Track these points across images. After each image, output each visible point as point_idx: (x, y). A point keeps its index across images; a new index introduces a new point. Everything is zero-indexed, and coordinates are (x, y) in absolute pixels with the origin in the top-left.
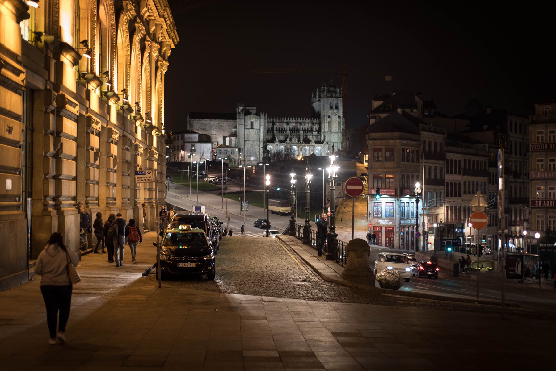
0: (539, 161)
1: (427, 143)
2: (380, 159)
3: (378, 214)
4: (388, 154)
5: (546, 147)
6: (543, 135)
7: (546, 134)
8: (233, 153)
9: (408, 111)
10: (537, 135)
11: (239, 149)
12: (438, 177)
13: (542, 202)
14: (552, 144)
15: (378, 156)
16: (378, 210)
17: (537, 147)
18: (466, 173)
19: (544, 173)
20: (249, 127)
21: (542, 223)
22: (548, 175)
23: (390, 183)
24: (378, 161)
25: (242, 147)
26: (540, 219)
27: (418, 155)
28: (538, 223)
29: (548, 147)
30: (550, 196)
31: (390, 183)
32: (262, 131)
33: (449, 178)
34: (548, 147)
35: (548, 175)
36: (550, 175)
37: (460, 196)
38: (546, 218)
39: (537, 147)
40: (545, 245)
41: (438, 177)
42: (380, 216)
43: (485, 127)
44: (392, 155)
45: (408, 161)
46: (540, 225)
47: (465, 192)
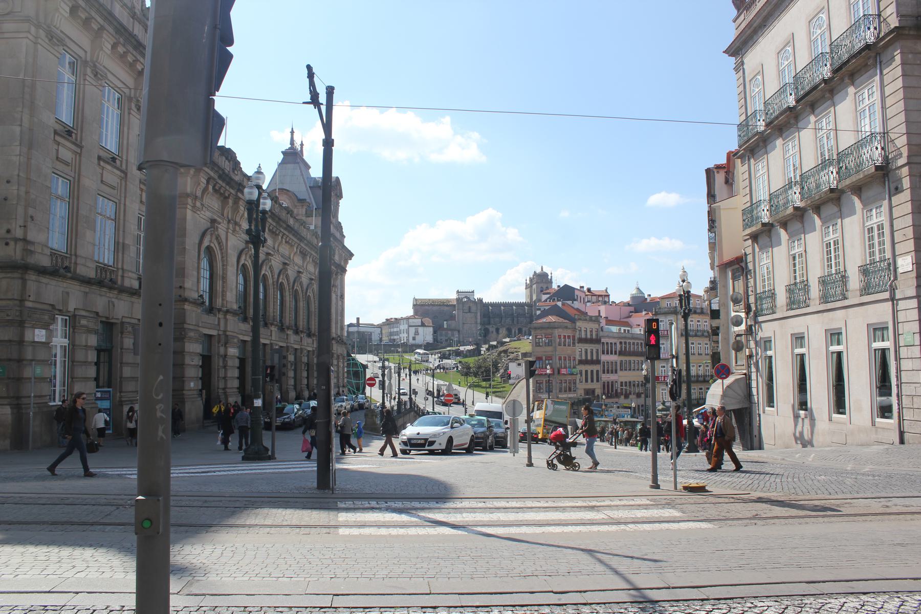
1: (583, 329)
8: (453, 335)
9: (570, 302)
12: (595, 358)
18: (621, 353)
27: (574, 339)
32: (479, 314)
33: (604, 358)
37: (616, 372)
41: (595, 358)
44: (550, 341)
45: (565, 345)
47: (621, 370)
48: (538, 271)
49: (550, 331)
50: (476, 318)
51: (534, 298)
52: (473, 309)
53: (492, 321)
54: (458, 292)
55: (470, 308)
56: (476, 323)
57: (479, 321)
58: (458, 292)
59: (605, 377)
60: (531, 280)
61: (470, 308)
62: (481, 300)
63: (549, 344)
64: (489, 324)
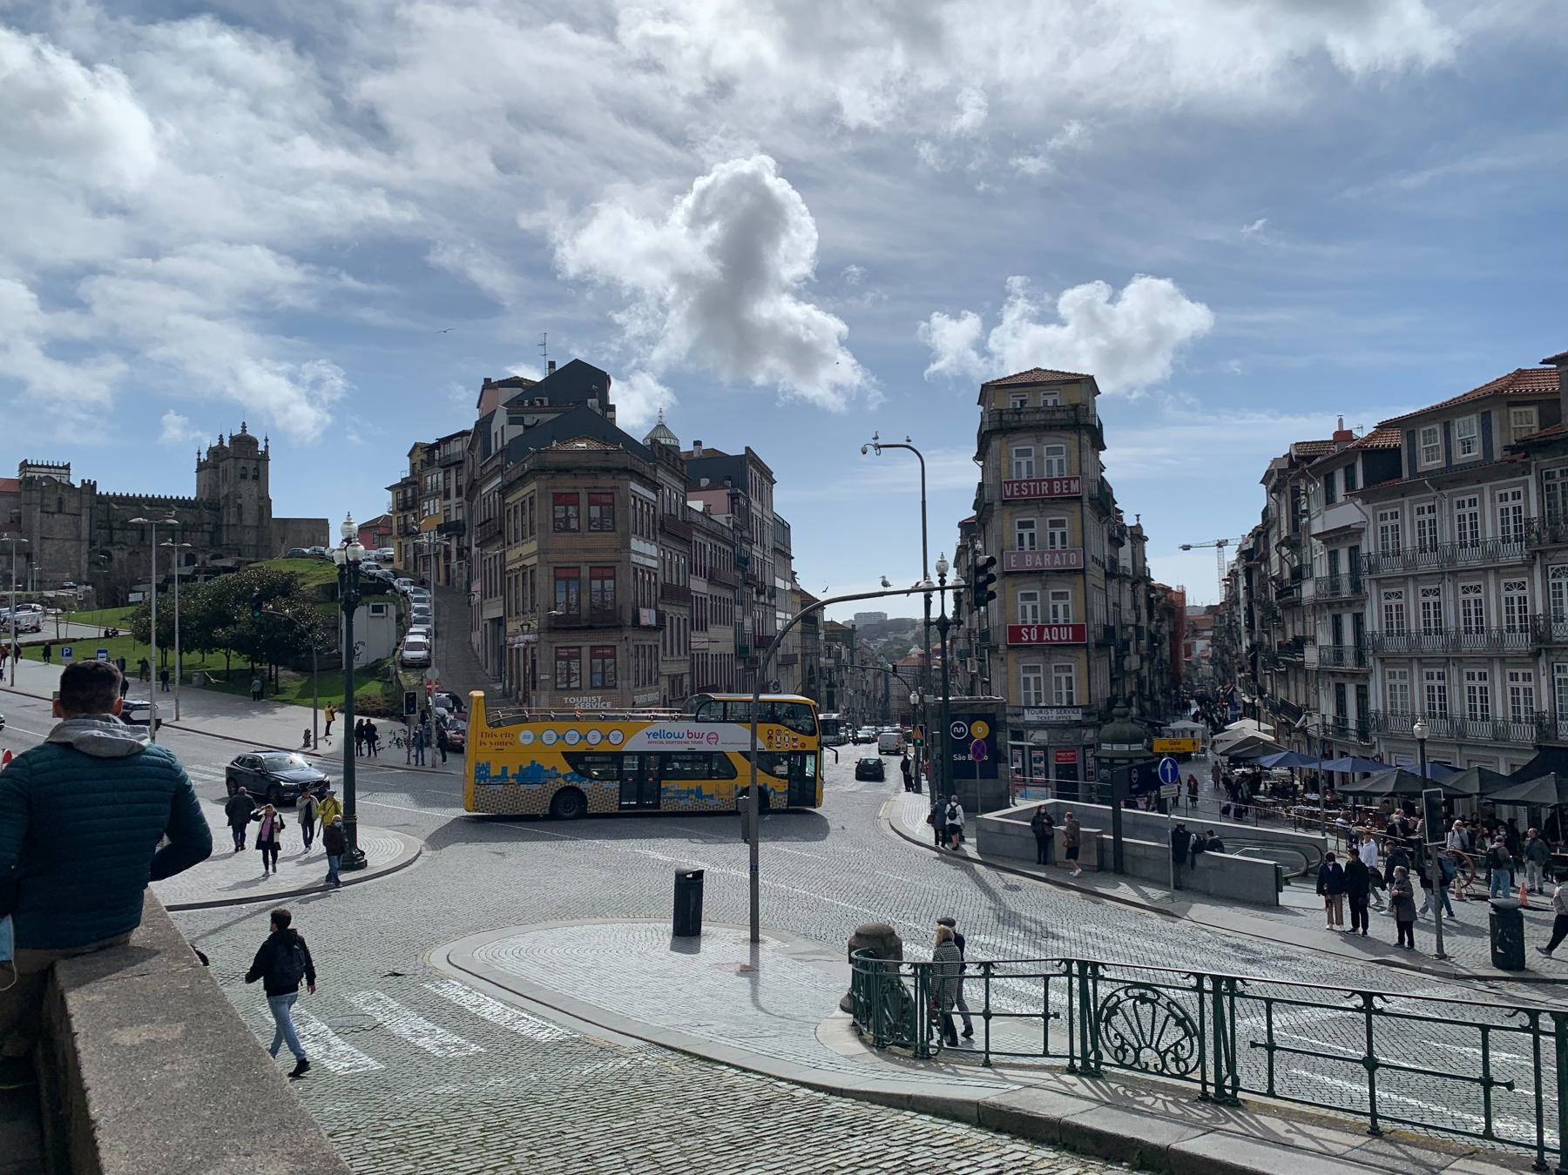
0: (1022, 525)
2: (574, 524)
3: (568, 682)
4: (595, 512)
5: (1045, 488)
6: (1032, 459)
7: (1039, 457)
10: (1015, 459)
11: (29, 556)
13: (1041, 630)
14: (1060, 480)
15: (568, 518)
16: (569, 668)
17: (1020, 490)
19: (1042, 557)
20: (53, 508)
21: (1038, 687)
22: (1053, 559)
23: (603, 590)
24: (567, 529)
25: (36, 550)
26: (1032, 677)
28: (1027, 686)
29: (1051, 489)
30: (1055, 614)
31: (603, 590)
32: (85, 519)
34: (1051, 489)
35: (1053, 559)
36: (1057, 561)
38: (1047, 672)
39: (1020, 490)
40: (1126, 747)
42: (575, 684)
43: (705, 482)
46: (1064, 691)
48: (237, 431)
49: (605, 482)
50: (78, 528)
51: (224, 491)
52: (72, 504)
53: (118, 535)
54: (24, 466)
55: (60, 501)
56: (78, 538)
57: (85, 533)
58: (24, 466)
59: (698, 640)
60: (213, 452)
61: (60, 501)
62: (90, 487)
63: (601, 526)
64: (111, 542)
